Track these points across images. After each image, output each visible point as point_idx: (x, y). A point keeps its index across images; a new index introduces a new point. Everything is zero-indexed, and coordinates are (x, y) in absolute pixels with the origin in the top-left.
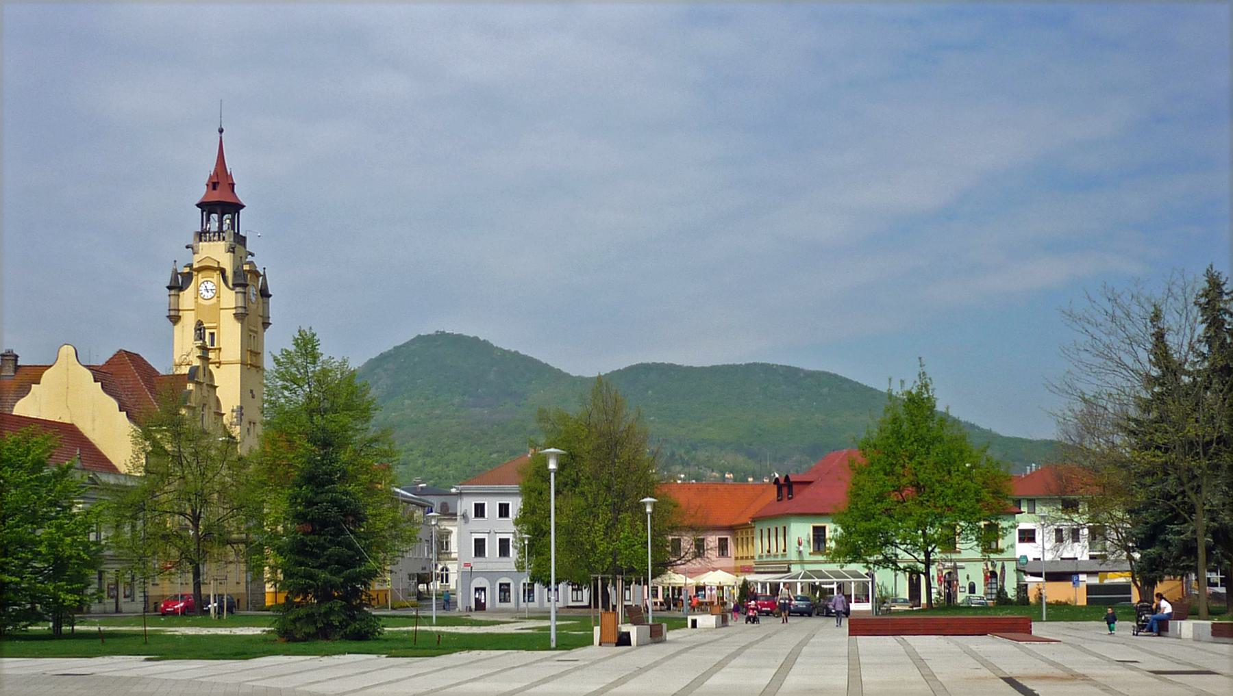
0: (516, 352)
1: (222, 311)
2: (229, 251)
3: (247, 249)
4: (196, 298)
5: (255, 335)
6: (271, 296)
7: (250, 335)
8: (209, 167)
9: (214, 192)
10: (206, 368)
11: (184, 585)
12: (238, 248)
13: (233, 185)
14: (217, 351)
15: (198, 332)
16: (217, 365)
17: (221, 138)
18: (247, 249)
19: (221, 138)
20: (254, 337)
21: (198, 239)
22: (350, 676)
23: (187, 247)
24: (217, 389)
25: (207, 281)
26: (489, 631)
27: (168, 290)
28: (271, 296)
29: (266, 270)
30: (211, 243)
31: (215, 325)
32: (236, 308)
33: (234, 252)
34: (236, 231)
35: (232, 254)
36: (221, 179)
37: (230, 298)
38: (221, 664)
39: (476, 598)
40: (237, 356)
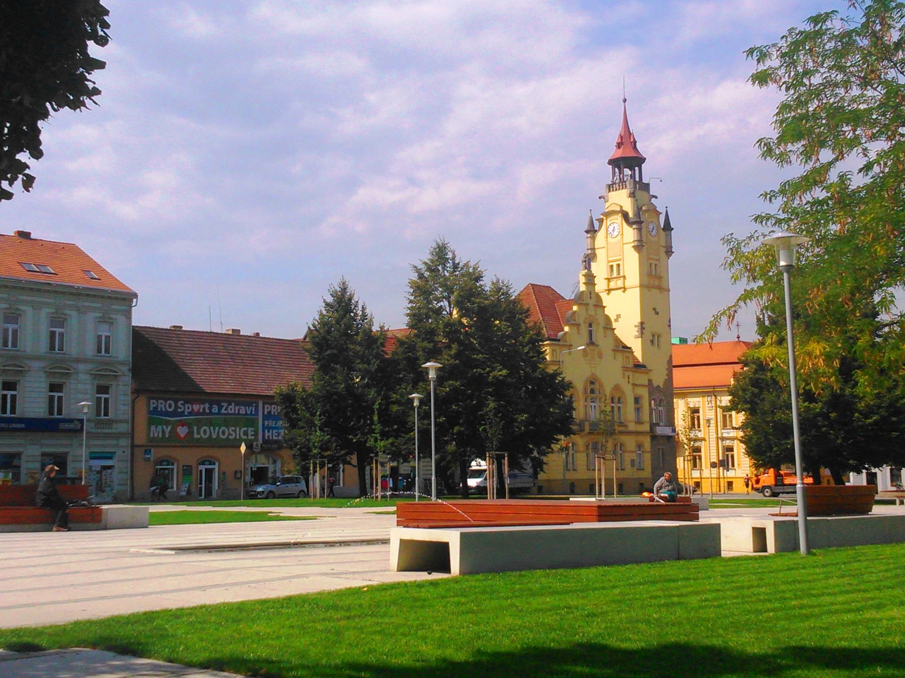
0: (25, 163)
1: (624, 246)
2: (630, 196)
3: (651, 194)
4: (607, 237)
5: (657, 262)
6: (673, 229)
7: (651, 264)
8: (614, 134)
9: (619, 150)
10: (592, 292)
11: (620, 470)
12: (639, 193)
13: (635, 142)
14: (622, 279)
15: (584, 263)
16: (623, 290)
17: (625, 106)
18: (651, 194)
19: (625, 106)
20: (656, 265)
21: (608, 191)
22: (345, 562)
23: (600, 198)
24: (606, 309)
25: (613, 223)
26: (518, 530)
27: (586, 234)
28: (673, 229)
29: (668, 209)
30: (617, 192)
31: (620, 257)
32: (634, 241)
33: (634, 197)
34: (637, 179)
35: (632, 199)
36: (627, 139)
37: (630, 234)
38: (102, 534)
39: (770, 496)
40: (636, 281)
